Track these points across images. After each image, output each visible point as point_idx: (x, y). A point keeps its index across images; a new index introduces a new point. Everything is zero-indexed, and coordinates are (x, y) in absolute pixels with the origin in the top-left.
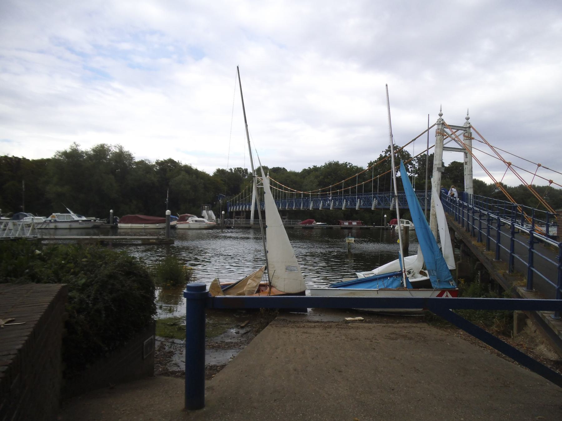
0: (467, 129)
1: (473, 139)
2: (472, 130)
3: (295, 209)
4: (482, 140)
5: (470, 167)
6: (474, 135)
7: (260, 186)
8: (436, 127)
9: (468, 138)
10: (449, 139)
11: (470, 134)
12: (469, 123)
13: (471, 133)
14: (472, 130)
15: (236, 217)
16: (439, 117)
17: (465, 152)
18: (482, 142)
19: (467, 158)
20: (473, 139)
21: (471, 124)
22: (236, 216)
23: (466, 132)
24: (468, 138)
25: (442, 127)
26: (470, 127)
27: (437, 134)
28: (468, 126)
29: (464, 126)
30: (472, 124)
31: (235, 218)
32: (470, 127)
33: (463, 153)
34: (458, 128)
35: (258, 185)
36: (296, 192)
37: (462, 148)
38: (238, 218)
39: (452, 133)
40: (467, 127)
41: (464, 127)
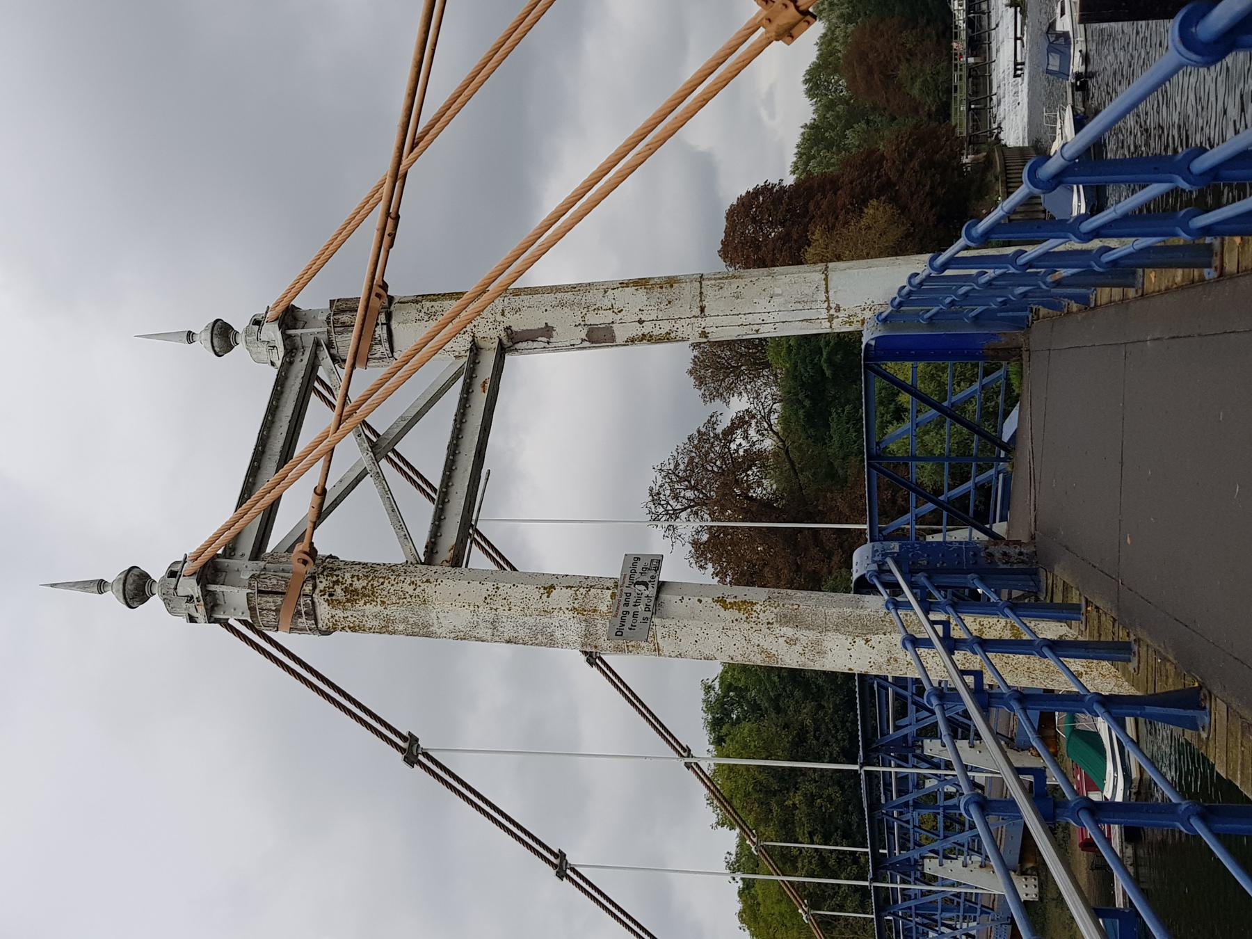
0: (306, 335)
2: (312, 301)
5: (634, 300)
9: (381, 332)
12: (257, 322)
13: (341, 307)
14: (312, 301)
16: (155, 602)
17: (502, 351)
19: (548, 331)
20: (378, 288)
28: (272, 332)
30: (266, 299)
33: (508, 357)
37: (460, 383)
40: (286, 337)
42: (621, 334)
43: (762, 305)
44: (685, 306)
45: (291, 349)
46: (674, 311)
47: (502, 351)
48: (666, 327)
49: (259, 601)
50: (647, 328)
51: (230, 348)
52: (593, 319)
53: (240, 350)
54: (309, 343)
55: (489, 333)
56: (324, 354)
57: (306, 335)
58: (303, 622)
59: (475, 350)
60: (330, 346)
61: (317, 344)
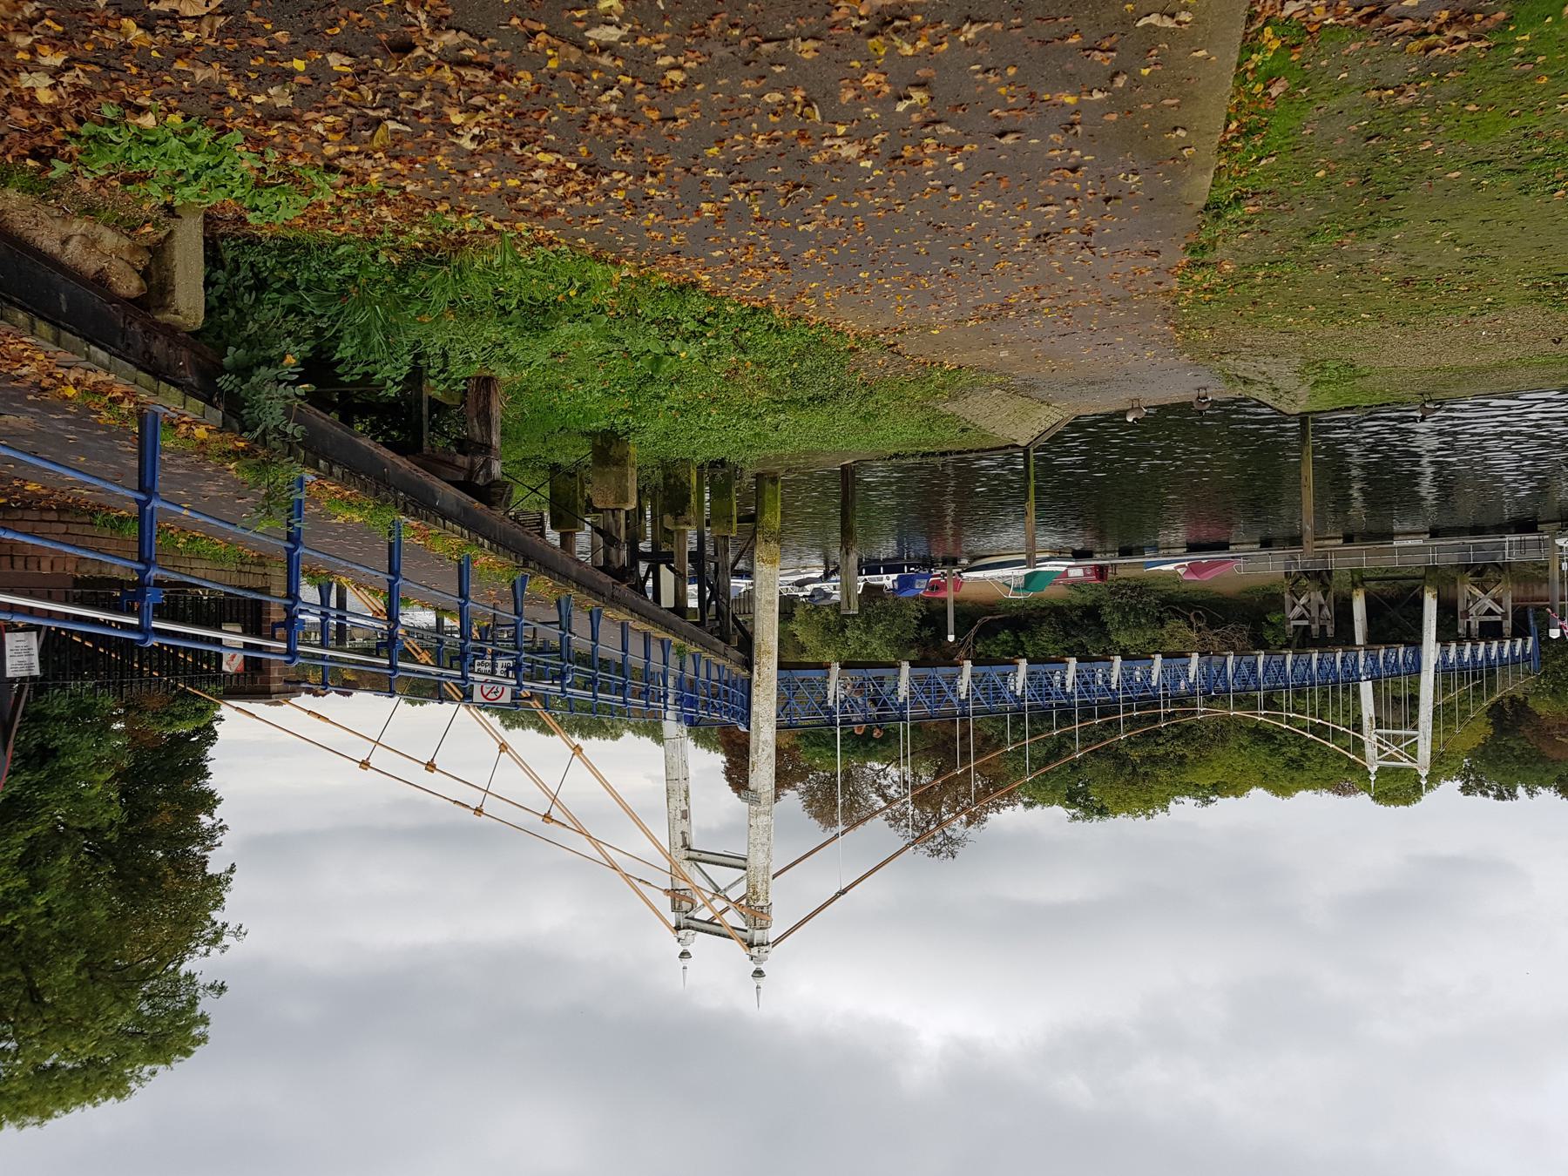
1: (667, 891)
2: (672, 919)
3: (1257, 652)
4: (639, 885)
6: (664, 903)
7: (1403, 732)
8: (772, 934)
9: (682, 892)
10: (734, 895)
11: (677, 905)
12: (679, 940)
13: (674, 909)
14: (672, 919)
15: (1499, 618)
17: (689, 849)
18: (640, 880)
19: (683, 833)
20: (667, 891)
21: (676, 939)
22: (1500, 623)
23: (687, 912)
24: (682, 892)
25: (753, 935)
26: (678, 928)
27: (765, 910)
28: (682, 933)
29: (693, 932)
30: (671, 936)
31: (1504, 615)
32: (678, 928)
34: (713, 928)
35: (1408, 738)
36: (1257, 714)
37: (699, 864)
38: (1490, 612)
39: (724, 916)
41: (693, 928)
42: (684, 807)
43: (675, 759)
44: (676, 785)
45: (689, 928)
46: (677, 789)
47: (689, 849)
48: (682, 792)
49: (758, 926)
50: (683, 798)
51: (688, 953)
52: (679, 817)
53: (689, 949)
54: (686, 921)
55: (684, 853)
56: (691, 914)
57: (683, 922)
58: (765, 910)
59: (688, 859)
60: (687, 912)
61: (687, 918)
